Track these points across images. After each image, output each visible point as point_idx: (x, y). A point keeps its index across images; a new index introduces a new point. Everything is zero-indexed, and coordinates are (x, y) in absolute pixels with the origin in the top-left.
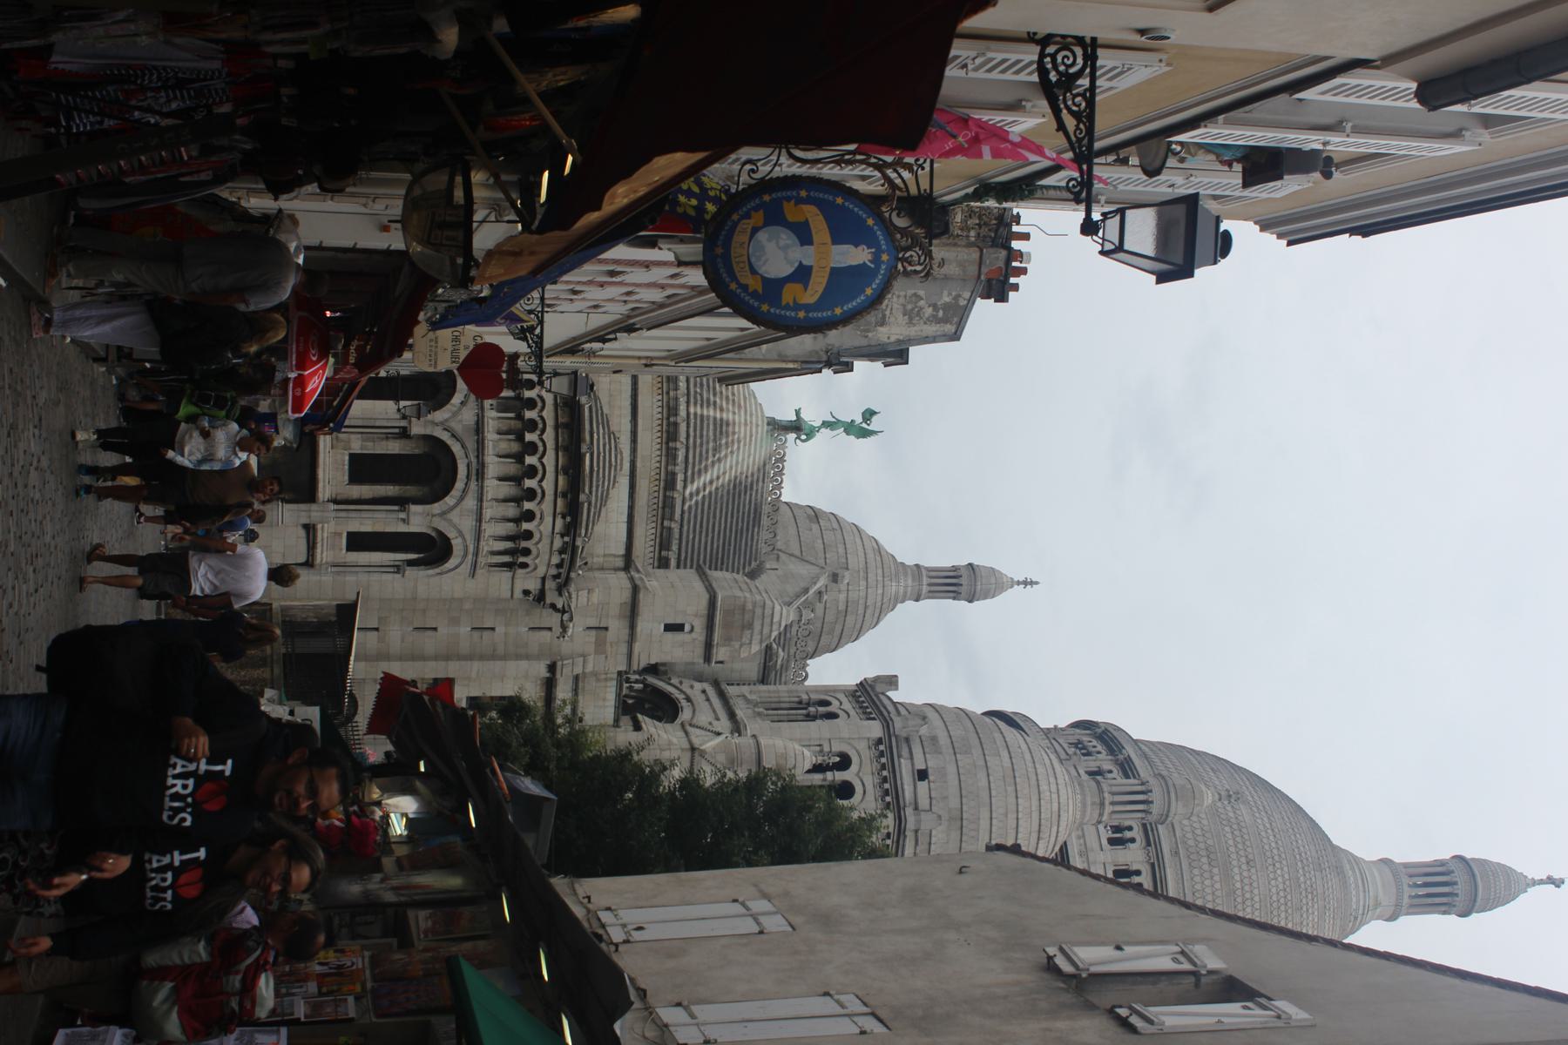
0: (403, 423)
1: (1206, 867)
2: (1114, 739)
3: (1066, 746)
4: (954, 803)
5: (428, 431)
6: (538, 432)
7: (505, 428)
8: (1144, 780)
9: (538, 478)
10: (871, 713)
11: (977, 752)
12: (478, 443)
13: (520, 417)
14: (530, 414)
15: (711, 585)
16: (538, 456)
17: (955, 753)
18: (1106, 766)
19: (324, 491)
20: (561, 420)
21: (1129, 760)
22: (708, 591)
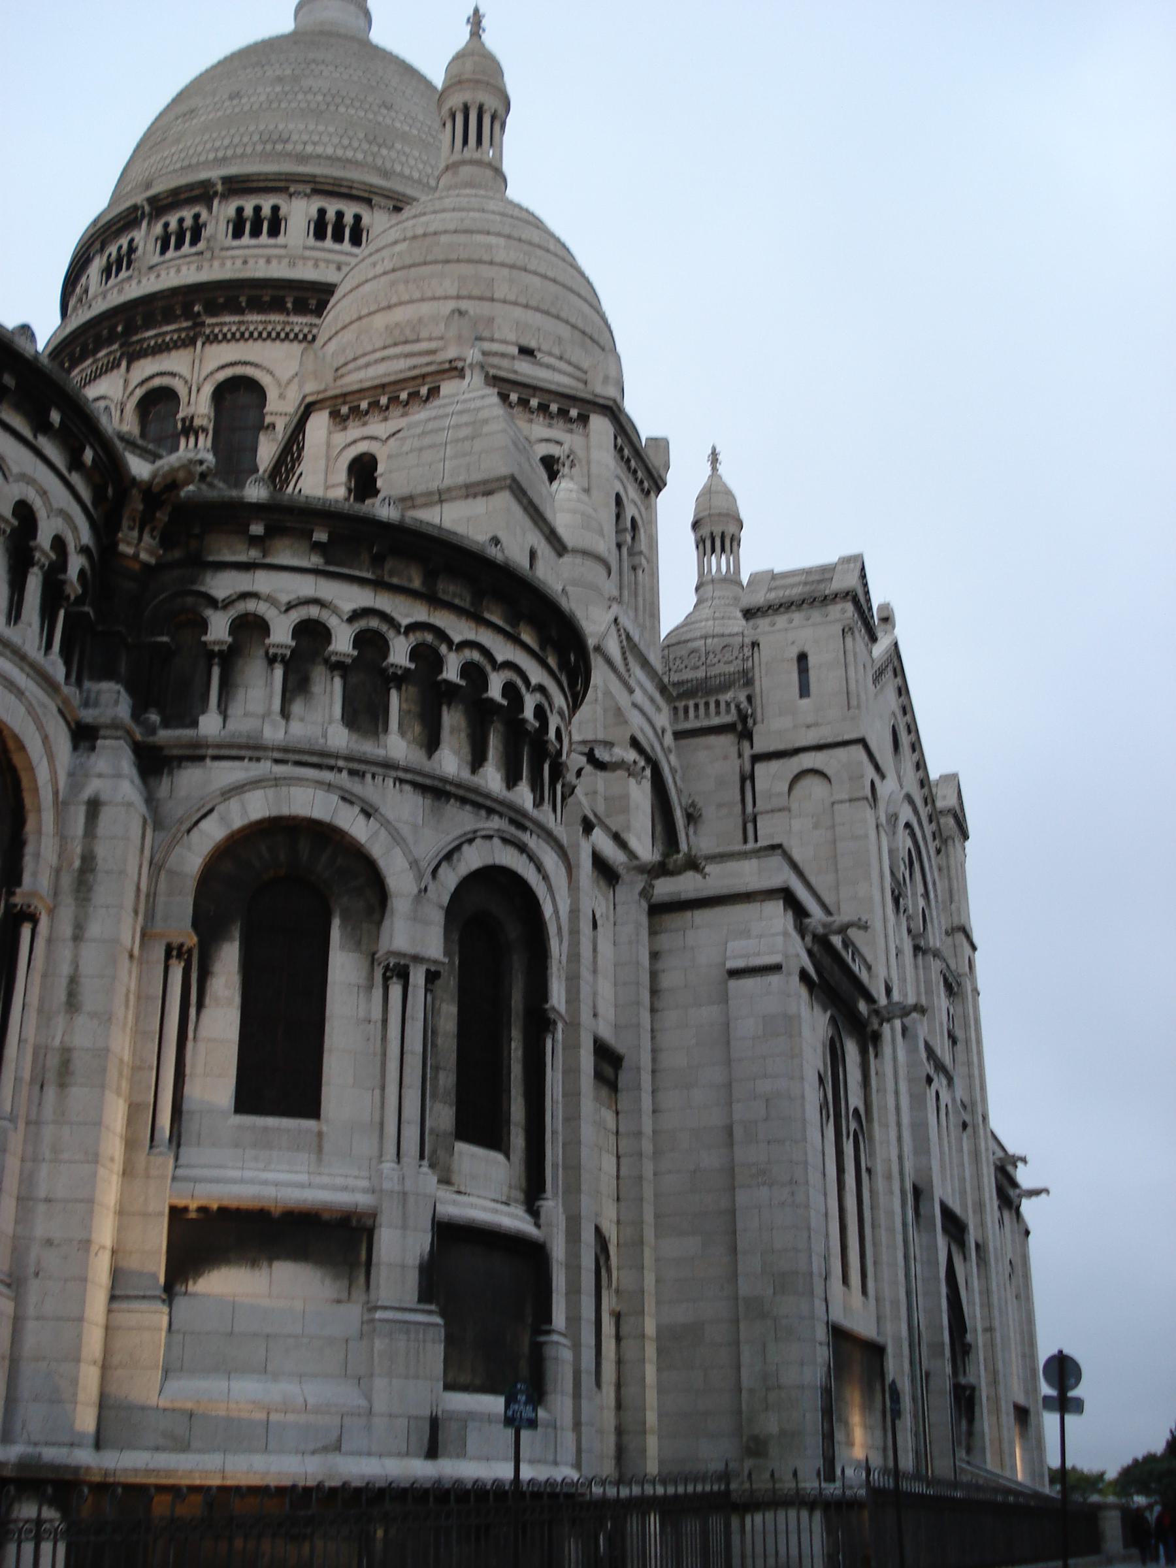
0: (418, 977)
1: (393, 154)
2: (176, 192)
3: (170, 254)
4: (565, 331)
5: (438, 917)
6: (443, 649)
7: (417, 729)
8: (461, 106)
9: (523, 689)
10: (414, 395)
11: (486, 271)
12: (464, 801)
13: (400, 679)
14: (399, 653)
15: (467, 486)
16: (488, 668)
17: (492, 300)
18: (230, 209)
19: (514, 1219)
20: (417, 584)
21: (227, 180)
22: (488, 493)
